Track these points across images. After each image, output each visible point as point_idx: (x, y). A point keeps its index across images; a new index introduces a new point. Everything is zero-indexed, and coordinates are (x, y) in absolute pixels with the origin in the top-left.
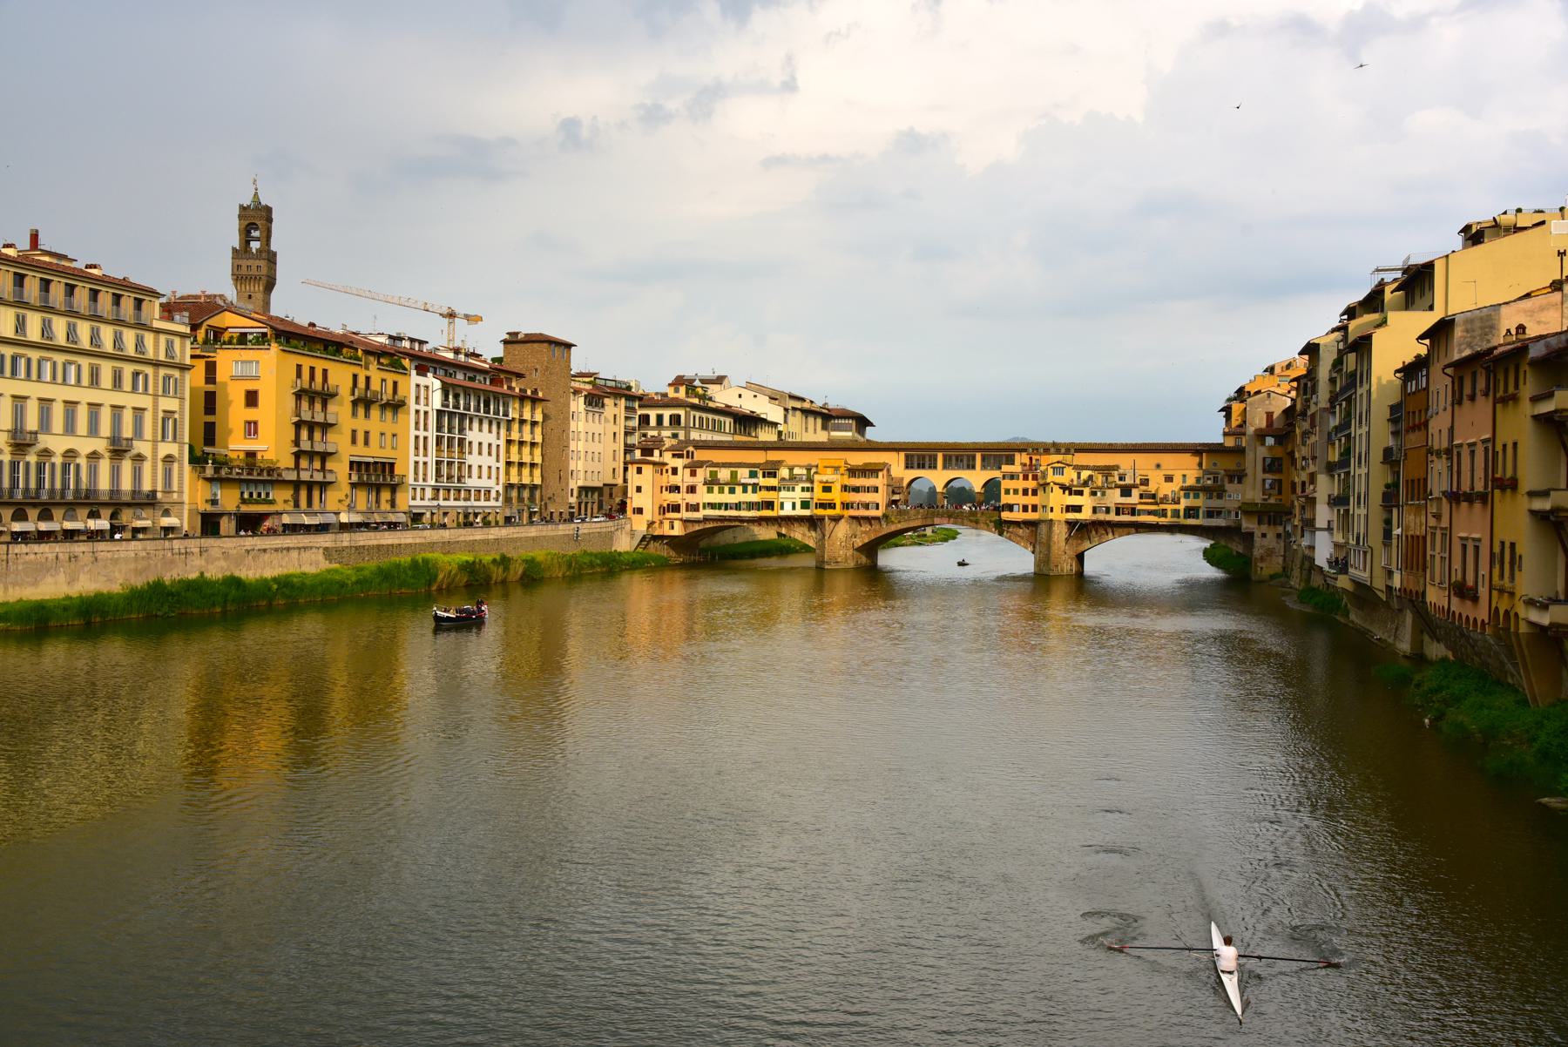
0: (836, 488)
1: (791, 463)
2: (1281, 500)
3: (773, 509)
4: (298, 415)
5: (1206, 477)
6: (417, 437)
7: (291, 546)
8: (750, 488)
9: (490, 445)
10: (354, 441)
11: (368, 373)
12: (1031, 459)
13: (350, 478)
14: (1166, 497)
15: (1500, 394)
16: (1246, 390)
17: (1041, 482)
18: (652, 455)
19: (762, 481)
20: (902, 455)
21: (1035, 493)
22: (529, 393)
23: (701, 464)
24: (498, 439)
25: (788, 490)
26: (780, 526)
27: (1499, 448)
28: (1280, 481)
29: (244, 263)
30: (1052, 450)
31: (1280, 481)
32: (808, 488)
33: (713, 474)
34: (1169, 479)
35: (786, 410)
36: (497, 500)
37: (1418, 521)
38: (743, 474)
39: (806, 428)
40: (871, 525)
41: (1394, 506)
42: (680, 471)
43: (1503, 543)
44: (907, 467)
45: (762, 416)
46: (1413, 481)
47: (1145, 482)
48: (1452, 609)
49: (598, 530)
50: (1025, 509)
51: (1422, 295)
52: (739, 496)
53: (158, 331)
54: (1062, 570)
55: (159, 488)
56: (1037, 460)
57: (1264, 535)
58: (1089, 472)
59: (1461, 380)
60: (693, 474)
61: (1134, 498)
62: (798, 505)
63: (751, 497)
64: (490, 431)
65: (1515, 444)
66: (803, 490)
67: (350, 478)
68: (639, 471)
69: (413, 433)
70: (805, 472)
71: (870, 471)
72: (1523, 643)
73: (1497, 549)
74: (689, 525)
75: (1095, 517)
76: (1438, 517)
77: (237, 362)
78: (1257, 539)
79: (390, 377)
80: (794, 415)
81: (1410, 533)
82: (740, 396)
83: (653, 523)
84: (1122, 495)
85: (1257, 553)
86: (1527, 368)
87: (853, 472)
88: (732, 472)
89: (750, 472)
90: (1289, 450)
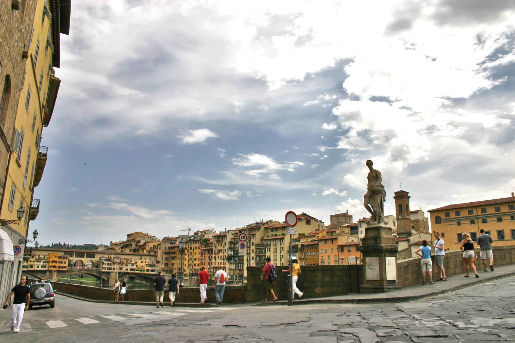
14: (141, 266)
17: (113, 262)
20: (63, 253)
21: (110, 265)
25: (38, 262)
26: (33, 273)
31: (167, 264)
34: (142, 262)
47: (136, 262)
50: (108, 269)
57: (167, 276)
58: (123, 260)
62: (40, 267)
66: (43, 262)
84: (132, 266)
87: (60, 258)
90: (173, 255)
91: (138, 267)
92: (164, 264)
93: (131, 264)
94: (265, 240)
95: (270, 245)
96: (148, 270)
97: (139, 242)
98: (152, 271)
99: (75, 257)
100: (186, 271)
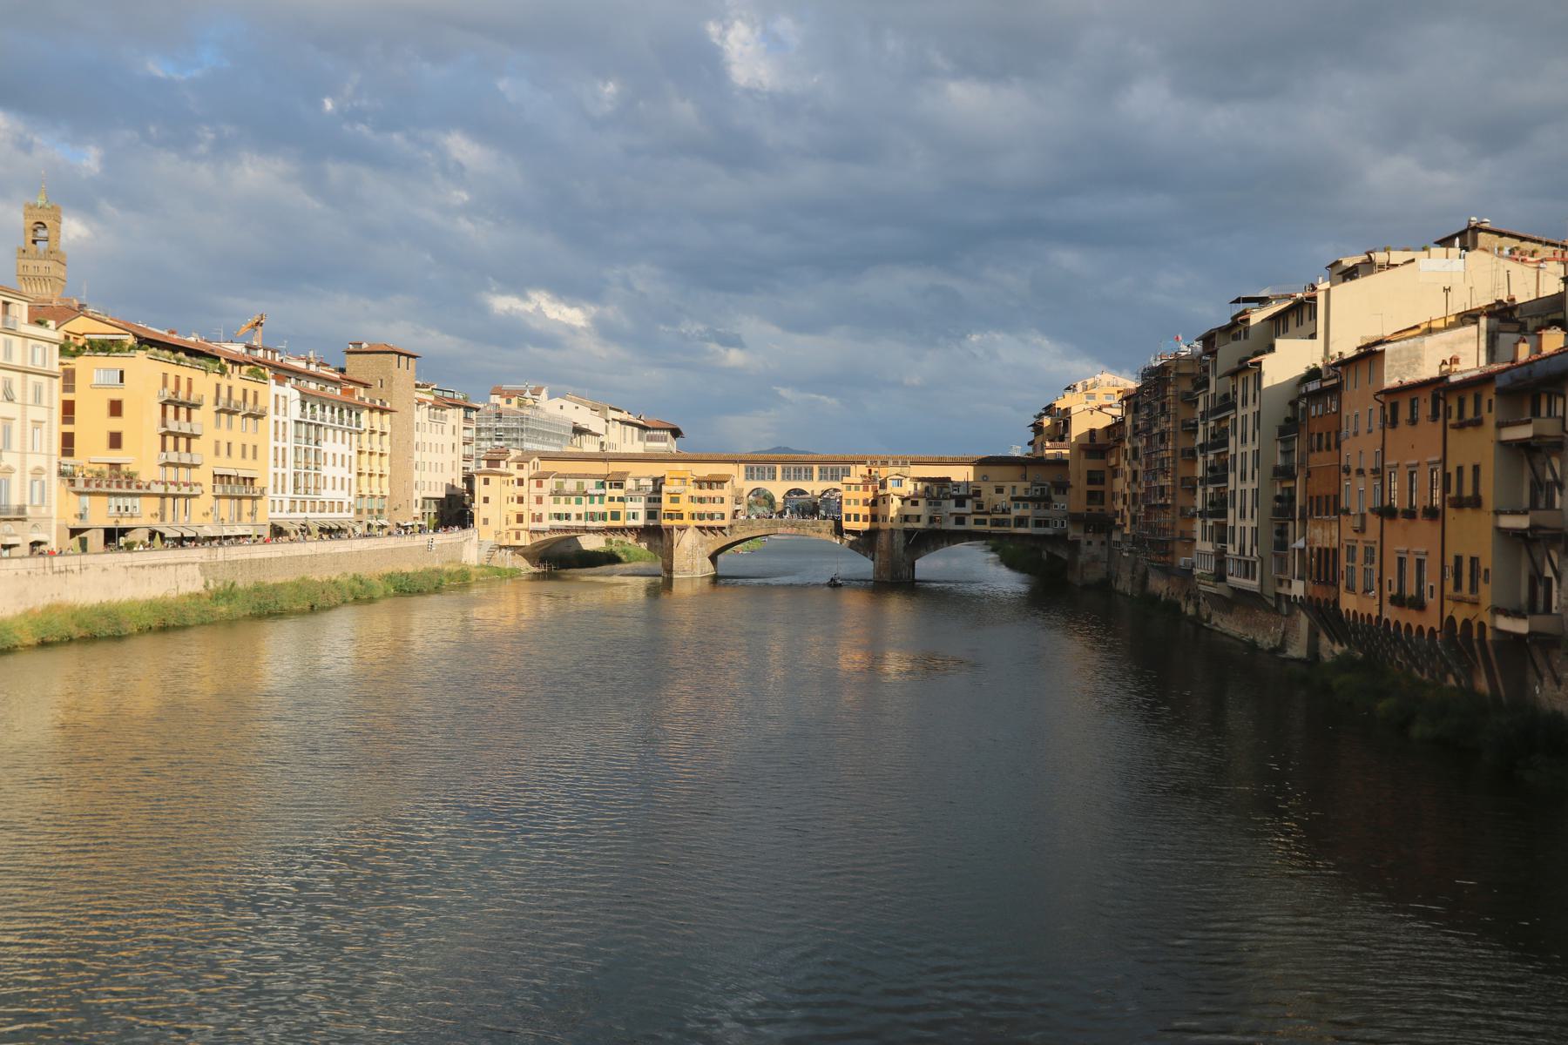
0: (684, 499)
1: (638, 474)
2: (1103, 510)
3: (619, 519)
4: (164, 425)
5: (1034, 488)
6: (276, 448)
7: (168, 561)
8: (597, 499)
9: (343, 456)
10: (217, 453)
11: (230, 383)
12: (870, 471)
13: (214, 491)
15: (1453, 420)
16: (1057, 406)
17: (881, 492)
18: (499, 467)
19: (611, 492)
22: (378, 403)
23: (545, 475)
24: (350, 449)
25: (635, 501)
27: (1452, 469)
28: (1102, 493)
29: (31, 263)
30: (891, 462)
31: (1102, 493)
32: (655, 499)
33: (560, 485)
34: (1000, 490)
35: (607, 421)
36: (349, 511)
37: (1327, 534)
38: (590, 485)
39: (625, 439)
40: (716, 535)
41: (1290, 520)
42: (526, 482)
43: (1458, 559)
44: (747, 479)
45: (585, 427)
46: (1317, 497)
47: (978, 493)
48: (1385, 616)
49: (450, 541)
51: (1299, 323)
52: (587, 507)
53: (26, 337)
54: (901, 578)
55: (27, 503)
56: (876, 472)
57: (1089, 543)
59: (1395, 407)
60: (539, 485)
61: (969, 506)
63: (597, 508)
64: (343, 442)
65: (1476, 469)
67: (214, 491)
68: (486, 482)
69: (273, 444)
70: (651, 483)
71: (719, 482)
72: (1490, 647)
73: (1450, 562)
74: (535, 535)
75: (931, 527)
76: (1362, 530)
77: (99, 369)
78: (1083, 546)
79: (252, 387)
80: (614, 427)
81: (1316, 546)
82: (562, 407)
83: (500, 533)
84: (956, 506)
85: (1081, 559)
86: (1493, 397)
87: (700, 483)
88: (578, 483)
89: (597, 482)
90: (1113, 461)
91: (984, 510)
92: (1084, 496)
93: (952, 497)
94: (1234, 374)
95: (1234, 406)
96: (1021, 521)
97: (1067, 411)
98: (1038, 524)
99: (783, 479)
100: (1125, 525)
